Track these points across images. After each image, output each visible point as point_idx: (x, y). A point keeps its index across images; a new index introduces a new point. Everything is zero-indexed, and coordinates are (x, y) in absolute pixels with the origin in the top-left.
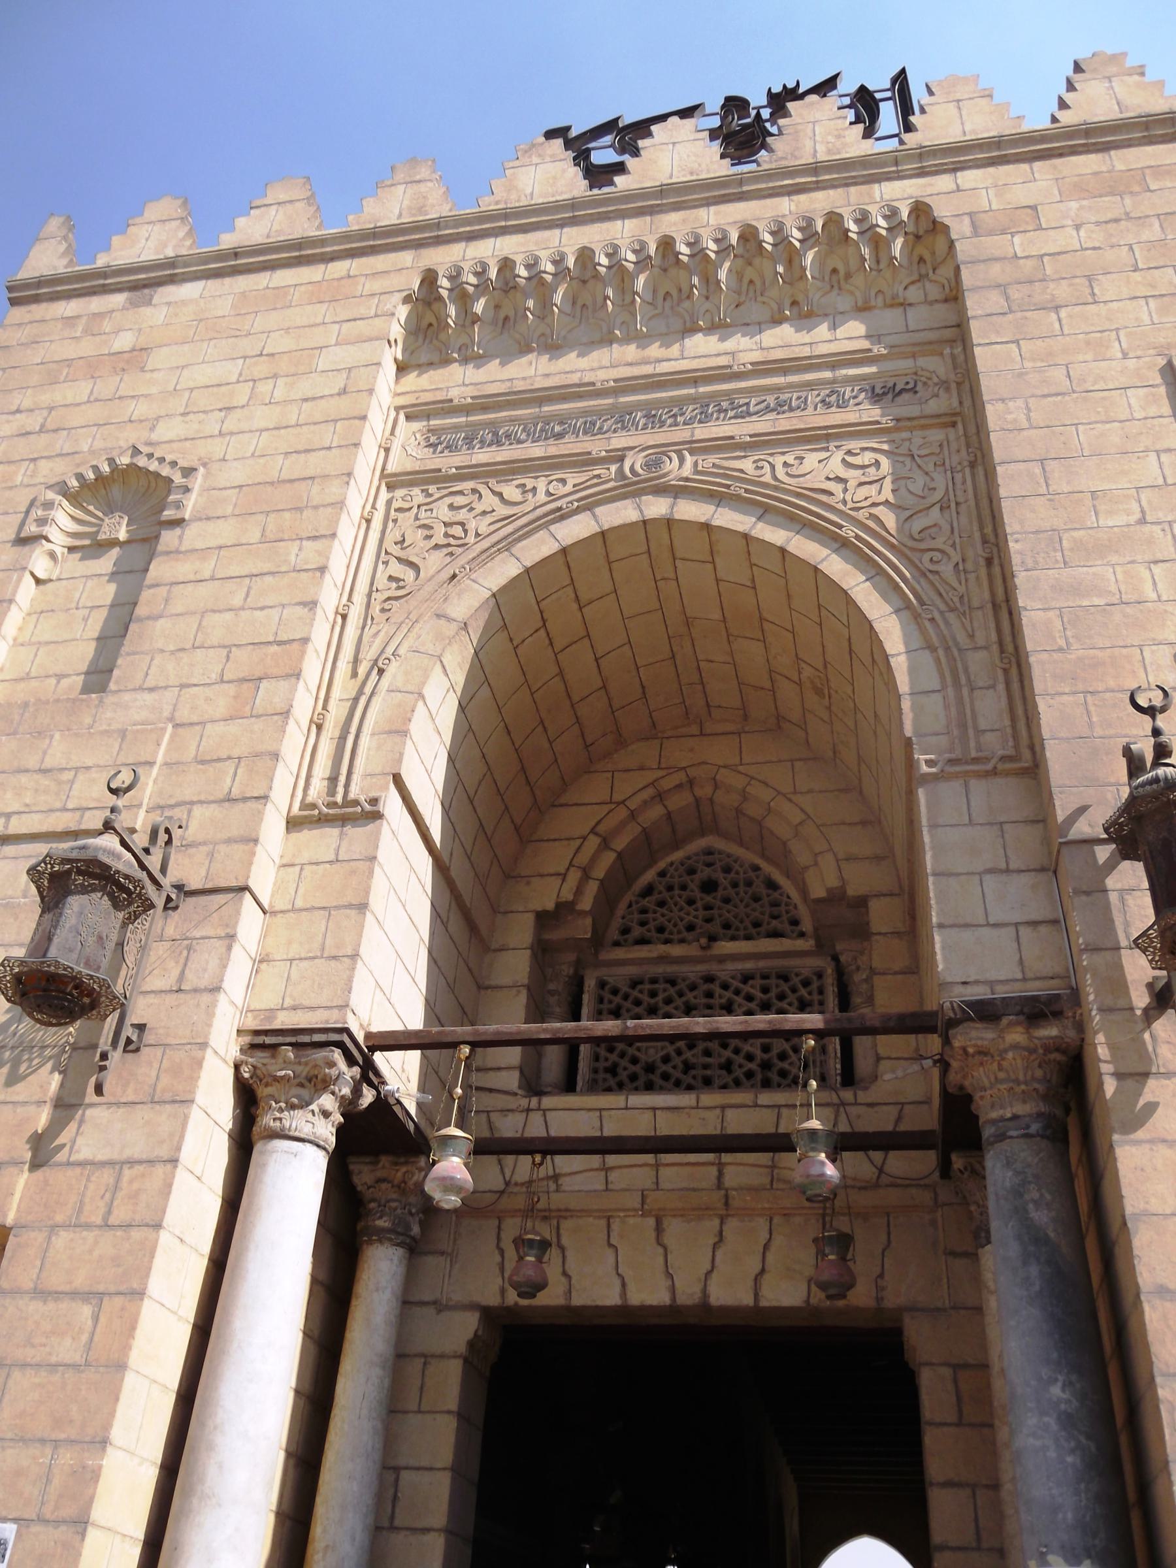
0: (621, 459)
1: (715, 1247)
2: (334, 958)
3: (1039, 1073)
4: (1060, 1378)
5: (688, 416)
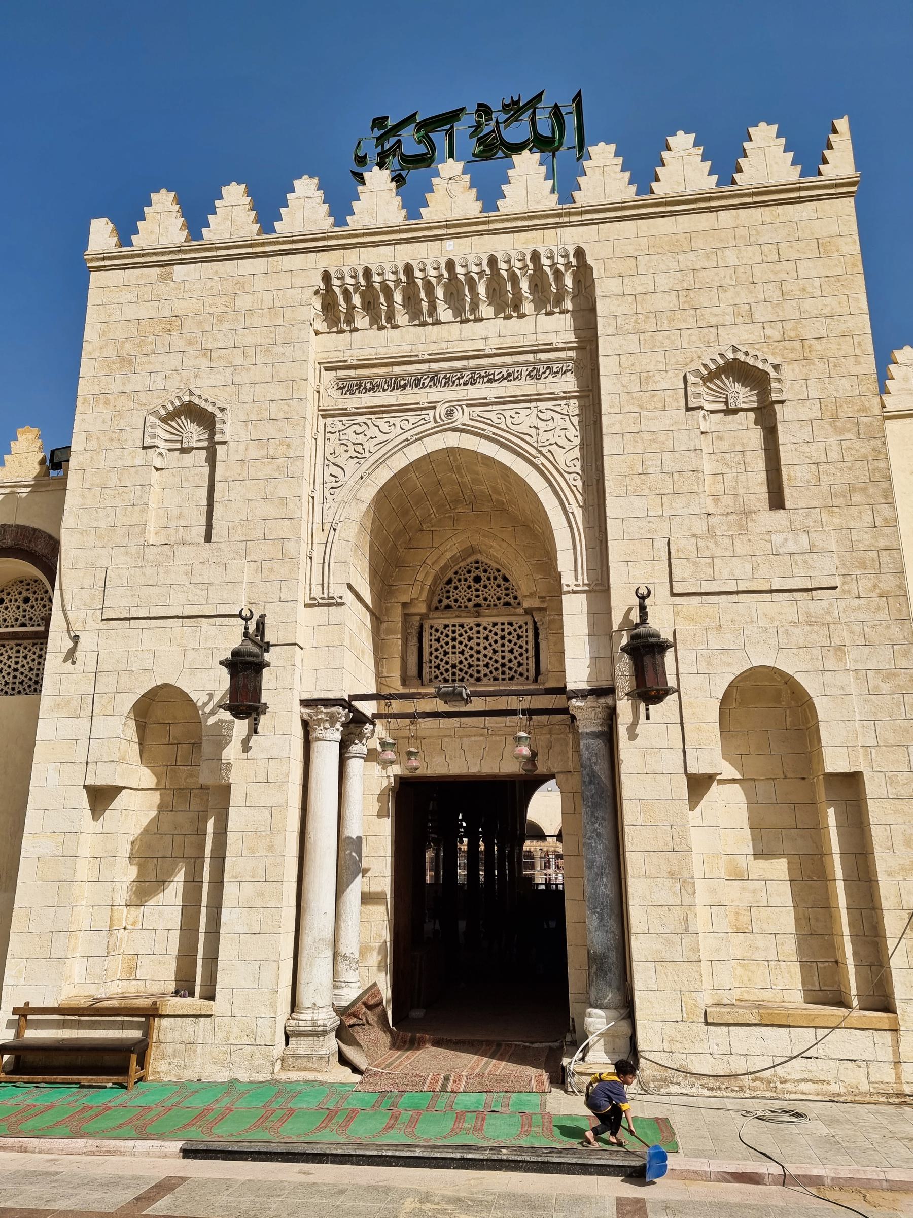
0: (434, 408)
3: (600, 715)
5: (465, 378)
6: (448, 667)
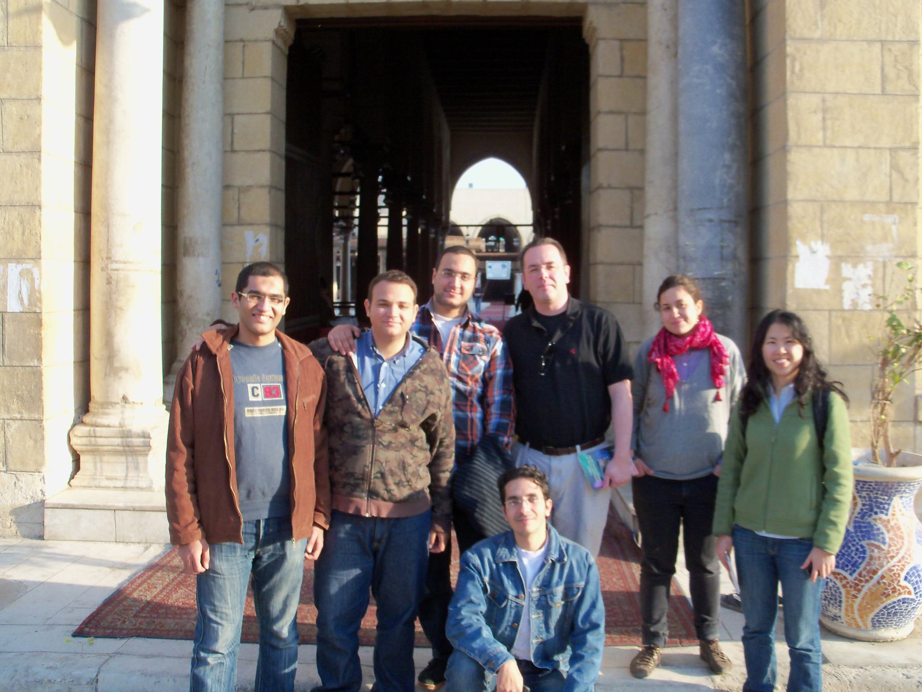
4: (719, 41)
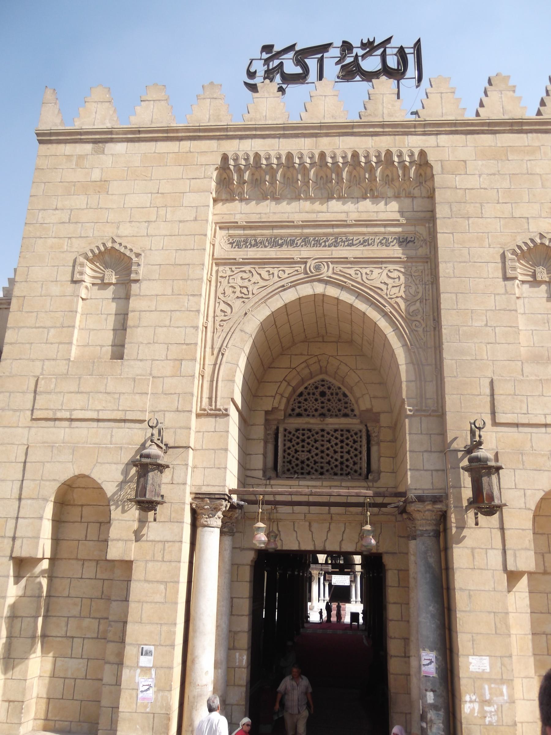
0: (306, 263)
1: (328, 532)
2: (219, 468)
3: (434, 517)
5: (330, 242)
6: (298, 462)
